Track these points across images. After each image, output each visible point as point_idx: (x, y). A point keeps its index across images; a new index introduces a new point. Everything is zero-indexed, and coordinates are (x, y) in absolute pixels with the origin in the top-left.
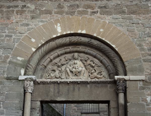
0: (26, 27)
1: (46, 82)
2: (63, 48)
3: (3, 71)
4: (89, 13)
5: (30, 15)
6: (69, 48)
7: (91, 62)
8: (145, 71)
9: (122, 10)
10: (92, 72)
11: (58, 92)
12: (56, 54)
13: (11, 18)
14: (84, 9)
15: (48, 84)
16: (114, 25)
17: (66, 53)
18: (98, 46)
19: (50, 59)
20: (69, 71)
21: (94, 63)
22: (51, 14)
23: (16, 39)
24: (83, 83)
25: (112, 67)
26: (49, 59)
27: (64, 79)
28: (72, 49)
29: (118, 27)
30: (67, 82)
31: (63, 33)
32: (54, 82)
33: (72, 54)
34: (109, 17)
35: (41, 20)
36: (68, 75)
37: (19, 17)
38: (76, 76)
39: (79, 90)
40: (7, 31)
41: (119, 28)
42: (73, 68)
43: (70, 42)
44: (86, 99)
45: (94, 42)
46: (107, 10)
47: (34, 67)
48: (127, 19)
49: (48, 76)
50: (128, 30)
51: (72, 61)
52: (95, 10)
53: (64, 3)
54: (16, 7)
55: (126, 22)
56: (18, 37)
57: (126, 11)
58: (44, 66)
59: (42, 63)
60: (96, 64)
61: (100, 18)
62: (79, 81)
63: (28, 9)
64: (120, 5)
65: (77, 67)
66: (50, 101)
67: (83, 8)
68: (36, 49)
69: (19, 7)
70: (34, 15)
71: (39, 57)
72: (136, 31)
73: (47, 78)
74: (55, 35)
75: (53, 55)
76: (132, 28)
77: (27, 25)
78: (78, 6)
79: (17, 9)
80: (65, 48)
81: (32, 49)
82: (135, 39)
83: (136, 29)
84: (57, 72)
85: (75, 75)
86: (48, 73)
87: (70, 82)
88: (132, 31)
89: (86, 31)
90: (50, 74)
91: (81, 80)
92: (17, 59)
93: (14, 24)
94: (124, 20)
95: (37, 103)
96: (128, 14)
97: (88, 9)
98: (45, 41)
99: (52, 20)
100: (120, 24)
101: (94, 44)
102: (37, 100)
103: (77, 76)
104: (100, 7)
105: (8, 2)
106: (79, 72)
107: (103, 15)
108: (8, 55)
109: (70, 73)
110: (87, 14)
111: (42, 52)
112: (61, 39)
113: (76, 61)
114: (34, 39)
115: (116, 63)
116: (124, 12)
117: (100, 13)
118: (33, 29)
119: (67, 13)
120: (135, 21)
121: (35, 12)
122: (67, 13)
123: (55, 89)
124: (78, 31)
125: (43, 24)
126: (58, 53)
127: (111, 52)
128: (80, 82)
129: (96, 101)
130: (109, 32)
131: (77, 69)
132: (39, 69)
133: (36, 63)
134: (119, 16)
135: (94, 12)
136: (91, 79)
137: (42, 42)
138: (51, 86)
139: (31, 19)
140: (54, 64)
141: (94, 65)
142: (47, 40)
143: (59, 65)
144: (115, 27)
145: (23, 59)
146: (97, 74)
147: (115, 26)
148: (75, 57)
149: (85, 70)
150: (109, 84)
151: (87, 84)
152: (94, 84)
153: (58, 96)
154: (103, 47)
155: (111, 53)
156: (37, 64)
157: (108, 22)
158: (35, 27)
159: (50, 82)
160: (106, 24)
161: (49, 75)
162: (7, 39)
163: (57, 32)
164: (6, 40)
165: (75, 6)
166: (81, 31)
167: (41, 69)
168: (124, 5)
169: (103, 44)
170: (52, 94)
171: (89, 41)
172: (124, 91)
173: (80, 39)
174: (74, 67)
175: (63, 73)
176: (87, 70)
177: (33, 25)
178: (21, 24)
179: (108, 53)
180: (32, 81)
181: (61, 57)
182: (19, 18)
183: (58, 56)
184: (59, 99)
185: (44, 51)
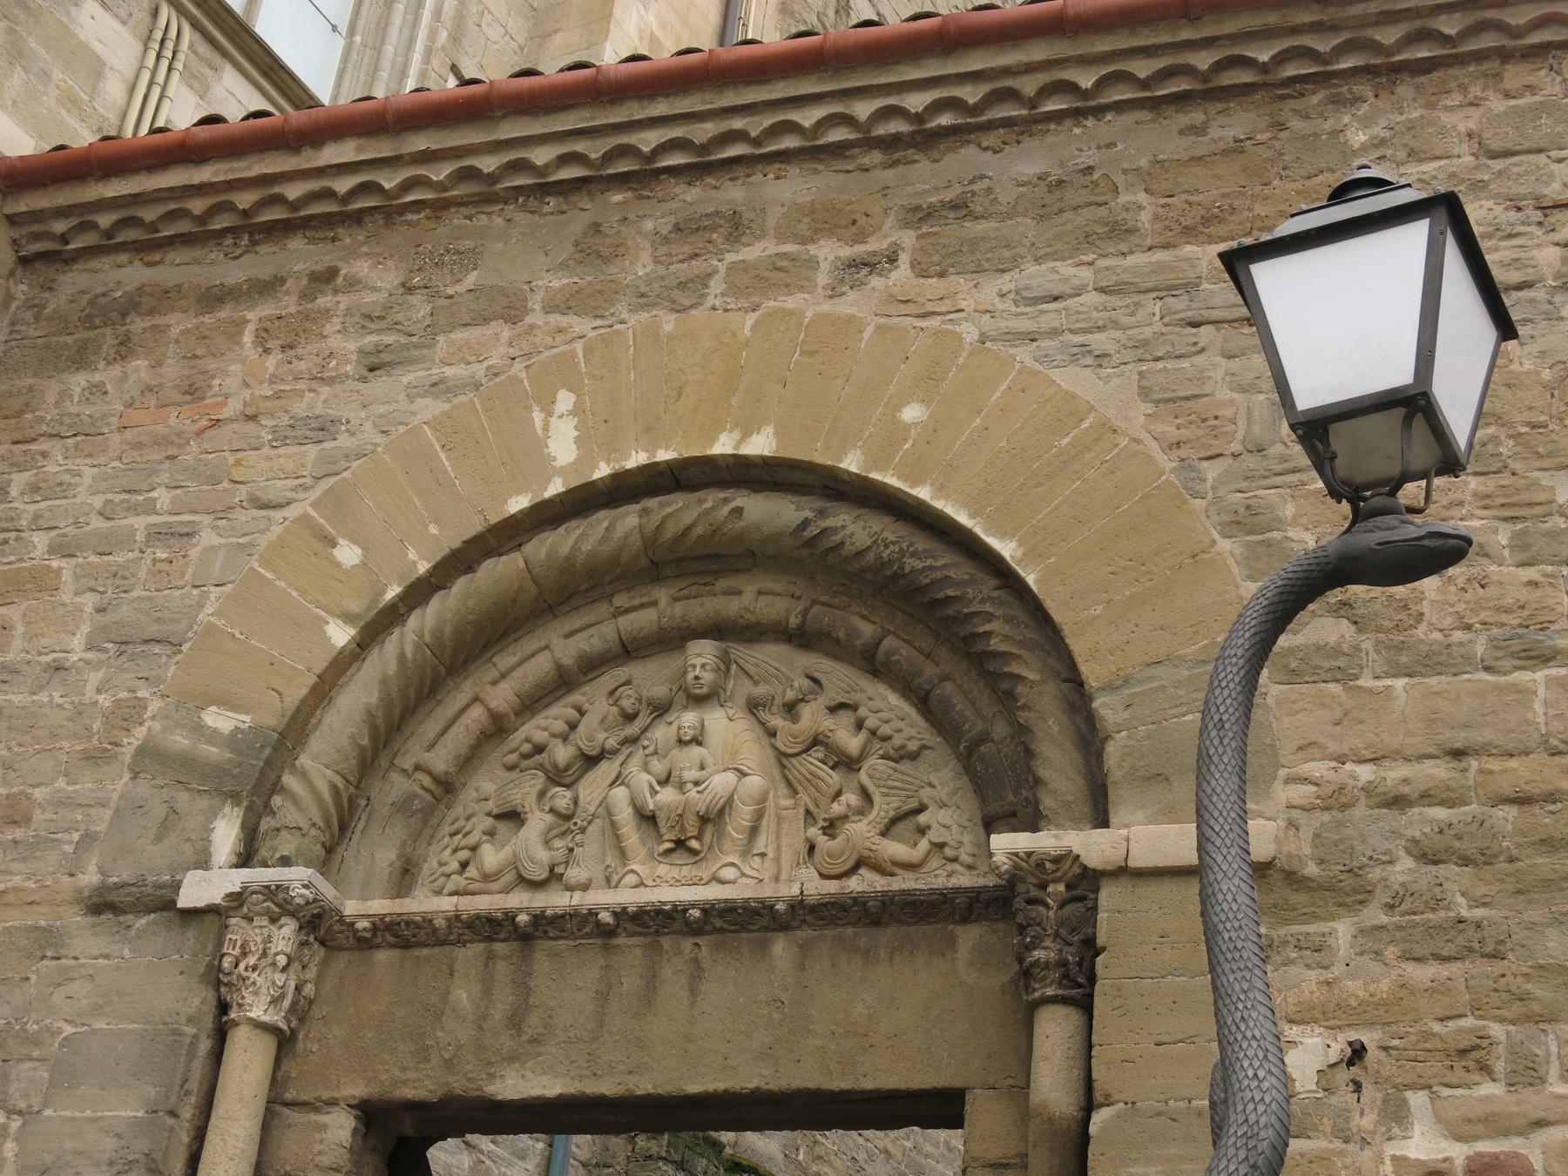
0: (312, 451)
1: (417, 925)
2: (603, 608)
3: (76, 837)
4: (823, 278)
5: (352, 346)
6: (654, 603)
8: (1282, 773)
9: (1103, 211)
10: (837, 808)
11: (516, 1021)
12: (540, 667)
13: (216, 382)
14: (790, 248)
16: (1023, 354)
17: (629, 650)
18: (883, 564)
19: (489, 710)
21: (859, 725)
22: (513, 320)
23: (221, 555)
24: (730, 917)
26: (477, 713)
27: (585, 887)
28: (678, 609)
29: (1055, 374)
30: (592, 913)
31: (595, 466)
34: (991, 290)
35: (435, 379)
36: (617, 853)
37: (271, 369)
38: (680, 857)
39: (693, 991)
40: (163, 497)
41: (1074, 380)
43: (650, 542)
44: (751, 1077)
45: (851, 528)
46: (981, 227)
48: (1143, 286)
49: (455, 865)
50: (1144, 393)
52: (875, 245)
53: (632, 216)
54: (260, 293)
55: (1133, 314)
56: (240, 540)
57: (1145, 218)
58: (430, 773)
59: (413, 752)
60: (873, 732)
61: (905, 309)
62: (693, 905)
63: (344, 301)
64: (1096, 176)
65: (691, 775)
66: (441, 1101)
67: (781, 238)
69: (288, 292)
70: (389, 339)
72: (1224, 394)
73: (450, 887)
74: (520, 498)
75: (517, 674)
76: (1185, 364)
77: (324, 429)
78: (737, 227)
79: (266, 309)
80: (620, 601)
81: (324, 632)
82: (1212, 471)
83: (1218, 374)
84: (538, 821)
85: (680, 844)
86: (460, 836)
87: (615, 914)
88: (1181, 394)
90: (474, 849)
91: (713, 893)
92: (199, 729)
93: (226, 431)
94: (1115, 301)
95: (323, 1128)
96: (1159, 240)
97: (813, 241)
98: (439, 557)
99: (518, 368)
100: (1078, 339)
101: (848, 549)
102: (326, 1095)
103: (695, 852)
104: (920, 216)
105: (212, 263)
106: (704, 820)
107: (942, 275)
108: (140, 694)
109: (632, 835)
110: (807, 286)
114: (355, 541)
115: (1025, 707)
116: (1120, 231)
117: (913, 267)
118: (360, 455)
119: (643, 295)
120: (1218, 301)
121: (400, 317)
122: (643, 299)
123: (487, 990)
124: (714, 440)
125: (447, 407)
127: (988, 608)
128: (704, 911)
129: (832, 1093)
131: (693, 793)
132: (386, 811)
134: (1073, 271)
135: (868, 265)
136: (823, 876)
137: (415, 563)
138: (459, 967)
139: (363, 379)
140: (526, 757)
141: (852, 743)
142: (457, 544)
143: (555, 766)
144: (1035, 374)
145: (247, 718)
146: (883, 834)
147: (1029, 362)
150: (965, 920)
151: (767, 929)
152: (829, 932)
153: (513, 1058)
154: (919, 565)
155: (990, 617)
158: (379, 439)
159: (448, 919)
161: (464, 854)
162: (155, 561)
163: (542, 466)
164: (142, 574)
165: (713, 229)
166: (736, 435)
167: (403, 806)
168: (1125, 166)
169: (921, 543)
170: (464, 1035)
171: (805, 523)
172: (1080, 986)
173: (726, 510)
175: (590, 830)
177: (368, 426)
178: (274, 430)
180: (283, 920)
181: (587, 688)
182: (272, 380)
183: (563, 682)
184: (513, 1086)
185: (427, 639)
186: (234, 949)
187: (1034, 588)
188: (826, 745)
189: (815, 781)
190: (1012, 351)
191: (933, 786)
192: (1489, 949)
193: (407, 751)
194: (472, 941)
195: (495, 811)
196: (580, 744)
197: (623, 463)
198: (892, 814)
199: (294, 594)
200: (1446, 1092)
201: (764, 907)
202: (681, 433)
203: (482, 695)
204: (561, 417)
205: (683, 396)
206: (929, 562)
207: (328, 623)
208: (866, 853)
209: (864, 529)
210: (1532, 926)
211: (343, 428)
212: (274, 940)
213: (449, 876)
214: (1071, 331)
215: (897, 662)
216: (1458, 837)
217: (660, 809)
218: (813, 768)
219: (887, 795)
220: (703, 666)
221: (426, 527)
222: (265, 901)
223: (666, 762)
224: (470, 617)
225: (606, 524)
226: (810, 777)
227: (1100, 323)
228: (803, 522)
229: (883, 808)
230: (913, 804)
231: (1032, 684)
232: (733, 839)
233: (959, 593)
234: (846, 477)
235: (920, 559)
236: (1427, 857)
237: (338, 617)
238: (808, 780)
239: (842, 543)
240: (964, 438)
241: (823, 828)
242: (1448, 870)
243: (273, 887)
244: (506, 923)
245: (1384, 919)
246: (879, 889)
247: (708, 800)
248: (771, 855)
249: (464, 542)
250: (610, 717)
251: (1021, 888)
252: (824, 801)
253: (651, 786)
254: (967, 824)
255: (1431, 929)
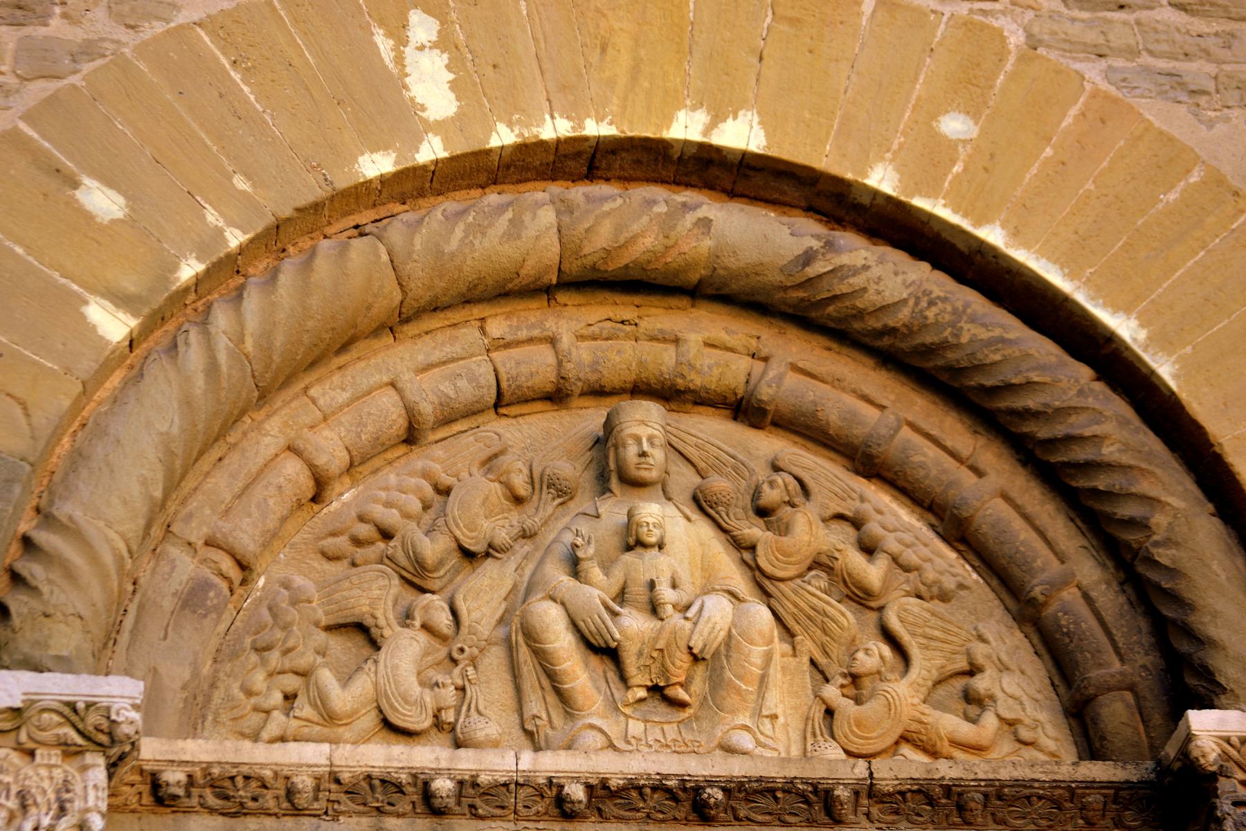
6: (552, 341)
7: (836, 525)
15: (297, 811)
16: (1093, 72)
19: (312, 467)
20: (562, 642)
21: (869, 549)
25: (1110, 598)
26: (293, 469)
27: (495, 744)
31: (490, 130)
32: (383, 781)
33: (591, 418)
36: (552, 698)
42: (622, 596)
45: (876, 271)
47: (108, 559)
49: (277, 698)
51: (583, 503)
60: (895, 559)
62: (711, 782)
65: (666, 594)
68: (135, 314)
71: (175, 430)
73: (273, 729)
74: (377, 157)
75: (345, 418)
81: (83, 317)
85: (656, 690)
87: (589, 788)
89: (769, 123)
90: (303, 674)
91: (737, 768)
94: (1199, 25)
100: (1162, 64)
101: (870, 299)
103: (682, 705)
111: (222, 358)
112: (448, 205)
113: (651, 511)
114: (109, 181)
115: (1168, 542)
124: (668, 120)
126: (412, 397)
127: (1090, 402)
130: (1048, 151)
131: (674, 619)
132: (168, 604)
133: (142, 509)
137: (219, 232)
142: (287, 212)
143: (420, 565)
144: (1116, 101)
147: (1104, 86)
148: (631, 452)
149: (771, 642)
154: (984, 334)
156: (142, 522)
157: (1016, 39)
159: (318, 779)
160: (1002, 60)
161: (292, 682)
171: (808, 258)
174: (638, 591)
176: (788, 633)
179: (1058, 410)
180: (89, 758)
181: (438, 451)
185: (249, 345)
186: (8, 797)
187: (1173, 384)
188: (829, 570)
189: (819, 618)
190: (1078, 66)
191: (981, 639)
193: (190, 516)
194: (349, 814)
195: (324, 621)
196: (458, 533)
197: (535, 130)
198: (935, 674)
199: (19, 250)
201: (816, 791)
202: (615, 100)
203: (300, 444)
204: (421, 48)
205: (610, 50)
206: (997, 332)
207: (86, 303)
208: (914, 726)
209: (896, 274)
211: (57, 10)
212: (78, 788)
213: (268, 712)
214: (1151, 53)
215: (922, 466)
217: (627, 638)
218: (815, 600)
219: (927, 648)
220: (651, 440)
221: (230, 179)
222: (60, 724)
223: (618, 575)
224: (310, 324)
225: (509, 215)
226: (812, 613)
227: (1187, 48)
228: (806, 252)
229: (924, 665)
230: (962, 664)
231: (1176, 513)
232: (738, 691)
233: (1048, 379)
234: (866, 201)
235: (984, 325)
237: (103, 296)
238: (809, 618)
239: (864, 290)
240: (1034, 170)
241: (842, 686)
243: (81, 706)
244: (409, 789)
246: (981, 776)
247: (706, 633)
248: (781, 720)
249: (298, 210)
250: (494, 499)
251: (1223, 784)
252: (836, 651)
253: (607, 608)
254: (1039, 696)
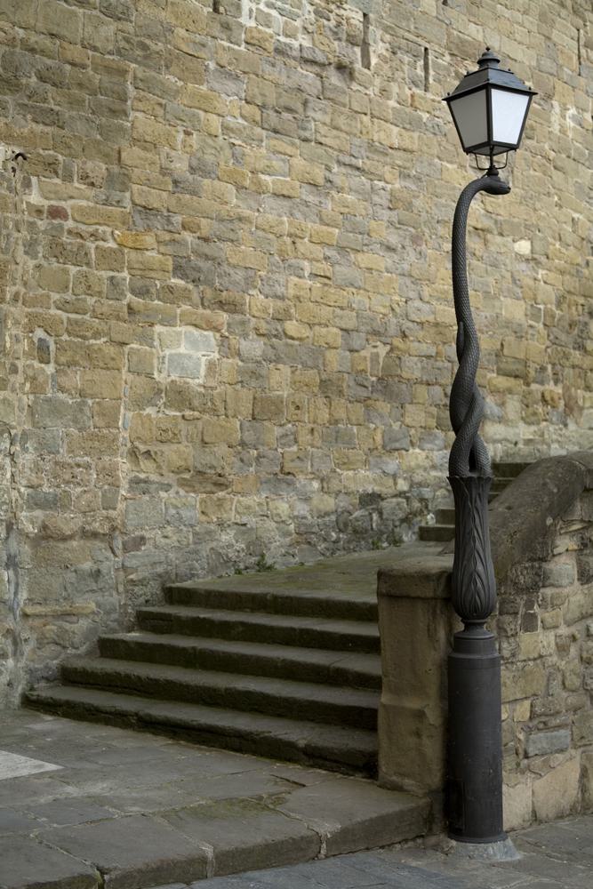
192: (61, 124)
200: (43, 179)
210: (71, 117)
216: (53, 74)
236: (42, 79)
242: (49, 87)
245: (26, 101)
255: (42, 110)
